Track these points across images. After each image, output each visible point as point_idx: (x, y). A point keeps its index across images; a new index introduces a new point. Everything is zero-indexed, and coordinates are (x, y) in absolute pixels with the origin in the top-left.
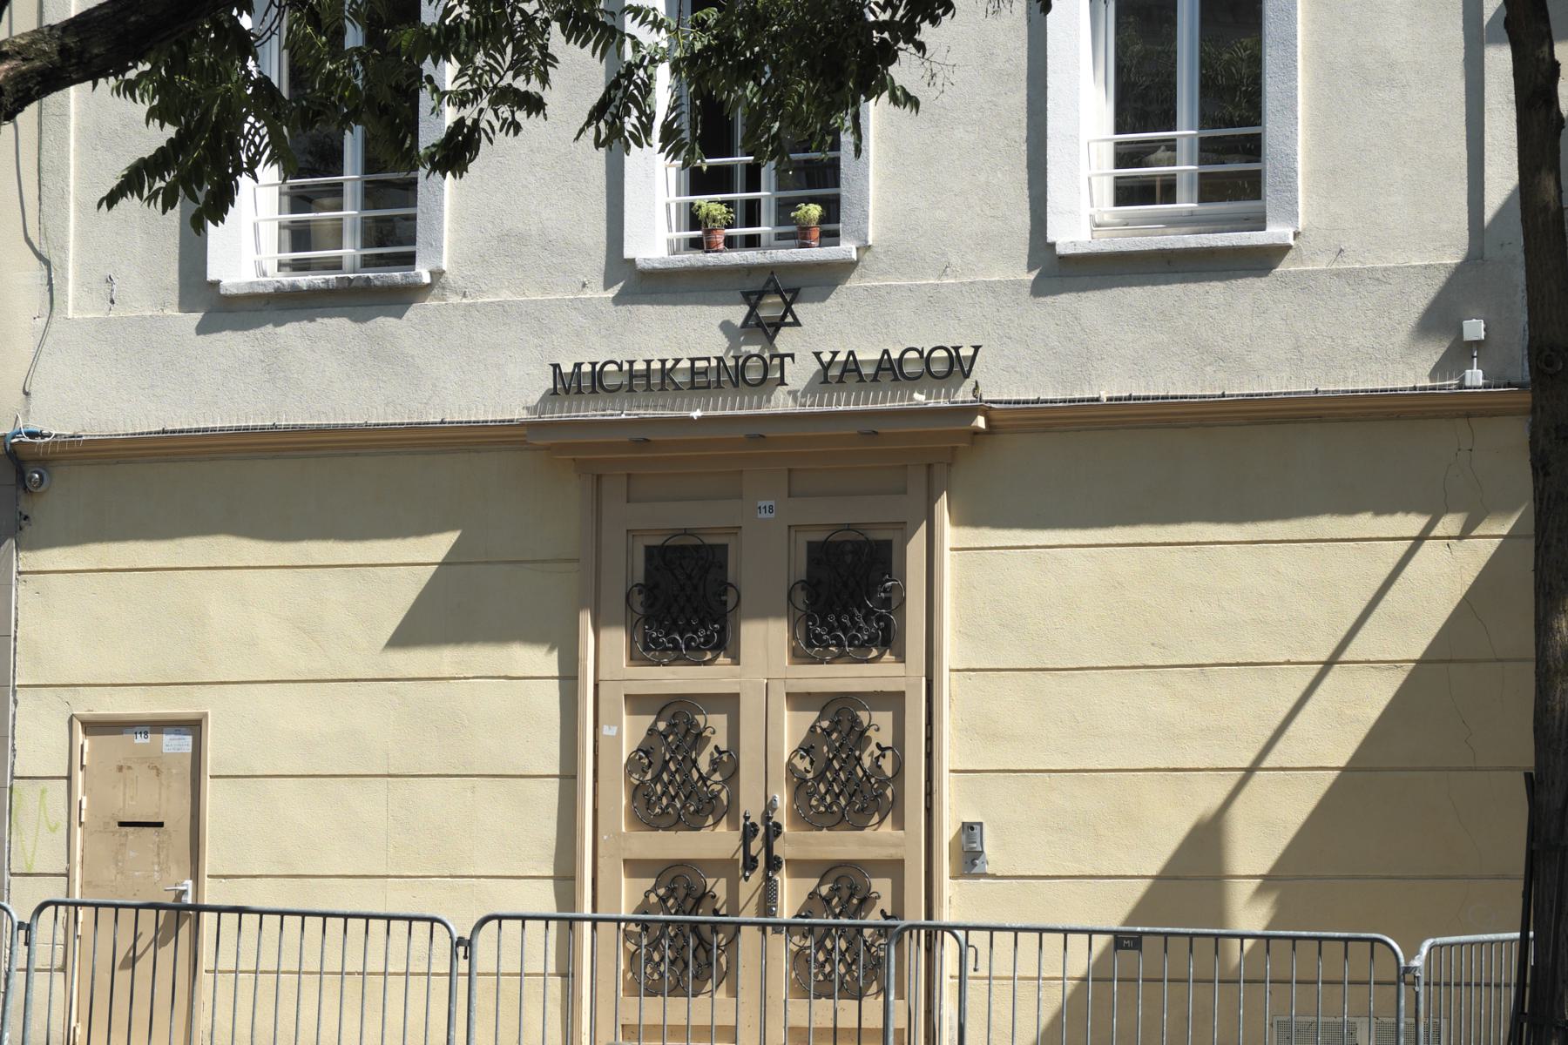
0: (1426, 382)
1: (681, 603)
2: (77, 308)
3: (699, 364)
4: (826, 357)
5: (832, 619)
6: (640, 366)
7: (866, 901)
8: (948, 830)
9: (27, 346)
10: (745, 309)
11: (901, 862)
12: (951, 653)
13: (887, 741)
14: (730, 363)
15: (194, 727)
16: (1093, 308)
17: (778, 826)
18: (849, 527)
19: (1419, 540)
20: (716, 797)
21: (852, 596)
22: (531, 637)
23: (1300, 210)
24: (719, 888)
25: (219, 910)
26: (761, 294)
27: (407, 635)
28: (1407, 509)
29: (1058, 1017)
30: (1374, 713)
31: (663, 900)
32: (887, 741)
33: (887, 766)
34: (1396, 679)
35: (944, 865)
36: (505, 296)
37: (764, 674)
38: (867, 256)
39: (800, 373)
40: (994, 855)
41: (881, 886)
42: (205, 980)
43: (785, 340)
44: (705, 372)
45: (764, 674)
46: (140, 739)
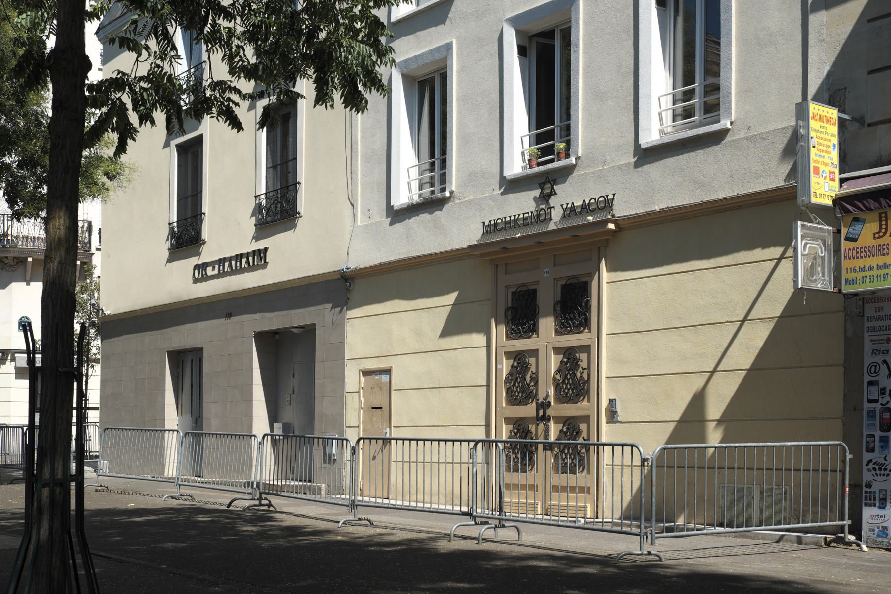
0: (782, 183)
1: (521, 316)
2: (362, 222)
3: (526, 215)
4: (565, 207)
5: (567, 316)
6: (508, 219)
7: (579, 433)
8: (604, 404)
9: (348, 237)
10: (539, 191)
11: (589, 417)
12: (605, 330)
13: (585, 366)
14: (535, 214)
15: (388, 371)
16: (655, 170)
17: (550, 403)
18: (573, 277)
19: (779, 260)
20: (532, 392)
21: (575, 307)
22: (478, 331)
23: (733, 112)
24: (532, 428)
25: (397, 439)
26: (544, 183)
27: (446, 332)
28: (775, 245)
29: (640, 488)
30: (761, 343)
31: (516, 434)
32: (585, 366)
33: (585, 376)
34: (770, 326)
35: (604, 419)
36: (471, 197)
37: (547, 334)
38: (579, 162)
39: (557, 215)
40: (621, 415)
41: (583, 427)
42: (393, 465)
43: (553, 201)
44: (527, 219)
45: (547, 334)
46: (376, 377)
